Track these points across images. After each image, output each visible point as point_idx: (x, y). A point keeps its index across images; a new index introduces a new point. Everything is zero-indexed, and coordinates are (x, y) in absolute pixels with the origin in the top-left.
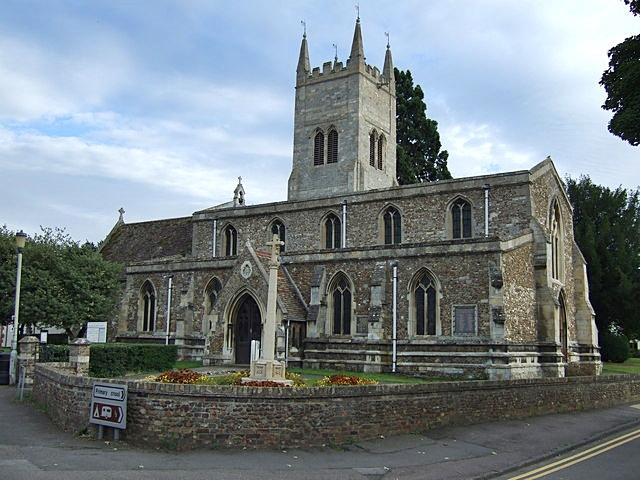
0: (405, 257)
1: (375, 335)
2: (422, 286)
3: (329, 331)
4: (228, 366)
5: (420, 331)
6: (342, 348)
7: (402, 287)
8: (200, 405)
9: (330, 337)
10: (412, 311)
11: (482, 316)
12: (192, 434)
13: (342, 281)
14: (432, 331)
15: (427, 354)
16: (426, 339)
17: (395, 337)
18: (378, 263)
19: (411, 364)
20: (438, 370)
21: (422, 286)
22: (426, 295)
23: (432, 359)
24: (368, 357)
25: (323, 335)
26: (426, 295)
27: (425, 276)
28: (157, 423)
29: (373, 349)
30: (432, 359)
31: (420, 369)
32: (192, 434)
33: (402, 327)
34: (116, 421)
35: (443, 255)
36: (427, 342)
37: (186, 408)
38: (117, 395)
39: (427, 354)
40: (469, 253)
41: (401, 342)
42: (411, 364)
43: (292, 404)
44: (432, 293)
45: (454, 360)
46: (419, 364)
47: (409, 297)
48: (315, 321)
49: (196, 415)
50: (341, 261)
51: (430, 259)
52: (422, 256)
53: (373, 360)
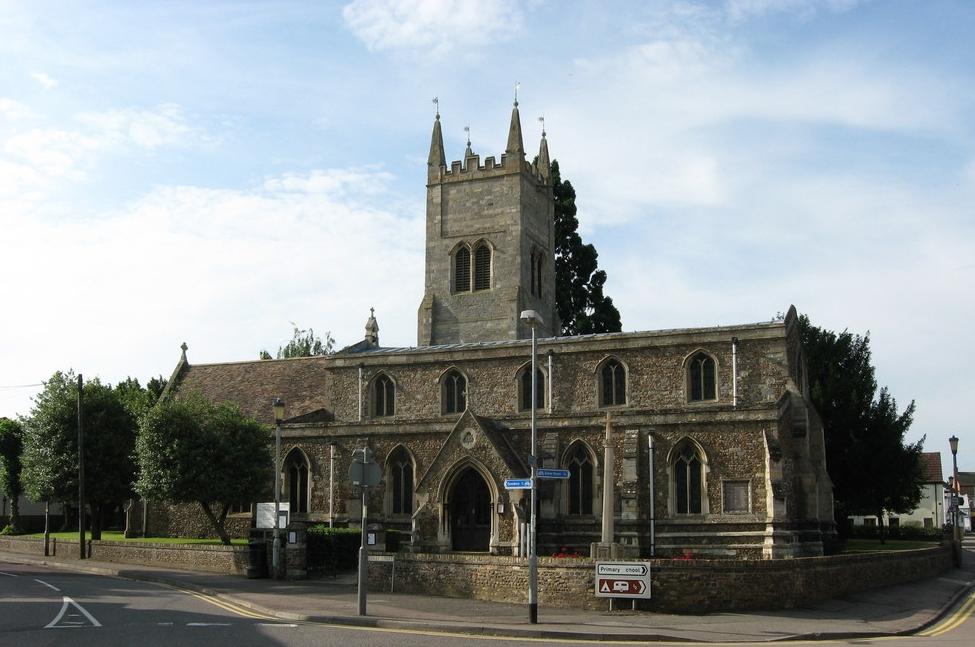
0: (663, 425)
1: (630, 514)
2: (684, 459)
3: (565, 510)
4: (445, 552)
5: (681, 508)
6: (583, 530)
7: (659, 460)
8: (709, 576)
9: (567, 517)
10: (671, 486)
11: (756, 491)
12: (704, 600)
13: (580, 450)
14: (697, 509)
15: (692, 534)
16: (691, 518)
17: (652, 516)
18: (628, 432)
19: (673, 546)
20: (707, 552)
21: (684, 459)
22: (688, 468)
23: (698, 540)
24: (622, 539)
25: (559, 515)
26: (688, 468)
27: (687, 448)
28: (672, 593)
29: (629, 530)
30: (698, 540)
31: (684, 551)
32: (704, 600)
33: (661, 505)
34: (637, 592)
35: (710, 423)
36: (692, 522)
37: (698, 579)
38: (637, 570)
39: (692, 534)
40: (741, 422)
41: (660, 522)
42: (673, 546)
43: (773, 573)
44: (696, 466)
45: (724, 540)
46: (682, 546)
47: (669, 471)
48: (552, 499)
49: (708, 584)
50: (579, 429)
51: (693, 428)
52: (684, 425)
53: (630, 542)
